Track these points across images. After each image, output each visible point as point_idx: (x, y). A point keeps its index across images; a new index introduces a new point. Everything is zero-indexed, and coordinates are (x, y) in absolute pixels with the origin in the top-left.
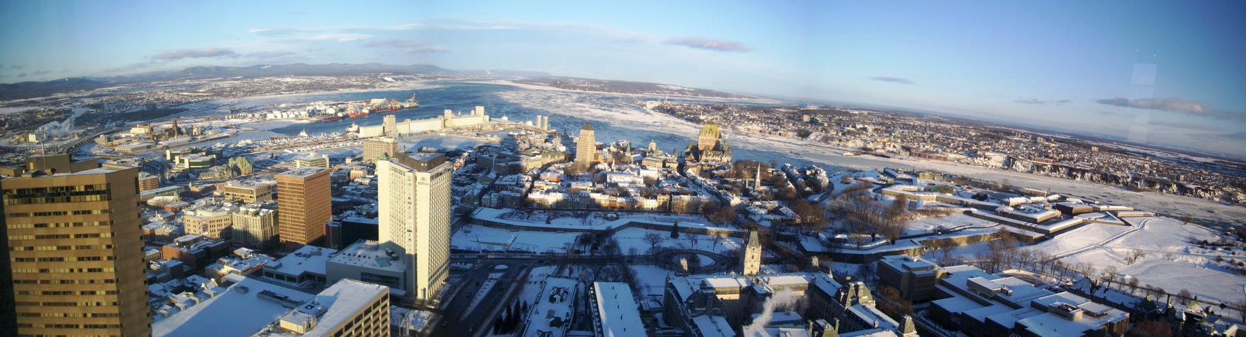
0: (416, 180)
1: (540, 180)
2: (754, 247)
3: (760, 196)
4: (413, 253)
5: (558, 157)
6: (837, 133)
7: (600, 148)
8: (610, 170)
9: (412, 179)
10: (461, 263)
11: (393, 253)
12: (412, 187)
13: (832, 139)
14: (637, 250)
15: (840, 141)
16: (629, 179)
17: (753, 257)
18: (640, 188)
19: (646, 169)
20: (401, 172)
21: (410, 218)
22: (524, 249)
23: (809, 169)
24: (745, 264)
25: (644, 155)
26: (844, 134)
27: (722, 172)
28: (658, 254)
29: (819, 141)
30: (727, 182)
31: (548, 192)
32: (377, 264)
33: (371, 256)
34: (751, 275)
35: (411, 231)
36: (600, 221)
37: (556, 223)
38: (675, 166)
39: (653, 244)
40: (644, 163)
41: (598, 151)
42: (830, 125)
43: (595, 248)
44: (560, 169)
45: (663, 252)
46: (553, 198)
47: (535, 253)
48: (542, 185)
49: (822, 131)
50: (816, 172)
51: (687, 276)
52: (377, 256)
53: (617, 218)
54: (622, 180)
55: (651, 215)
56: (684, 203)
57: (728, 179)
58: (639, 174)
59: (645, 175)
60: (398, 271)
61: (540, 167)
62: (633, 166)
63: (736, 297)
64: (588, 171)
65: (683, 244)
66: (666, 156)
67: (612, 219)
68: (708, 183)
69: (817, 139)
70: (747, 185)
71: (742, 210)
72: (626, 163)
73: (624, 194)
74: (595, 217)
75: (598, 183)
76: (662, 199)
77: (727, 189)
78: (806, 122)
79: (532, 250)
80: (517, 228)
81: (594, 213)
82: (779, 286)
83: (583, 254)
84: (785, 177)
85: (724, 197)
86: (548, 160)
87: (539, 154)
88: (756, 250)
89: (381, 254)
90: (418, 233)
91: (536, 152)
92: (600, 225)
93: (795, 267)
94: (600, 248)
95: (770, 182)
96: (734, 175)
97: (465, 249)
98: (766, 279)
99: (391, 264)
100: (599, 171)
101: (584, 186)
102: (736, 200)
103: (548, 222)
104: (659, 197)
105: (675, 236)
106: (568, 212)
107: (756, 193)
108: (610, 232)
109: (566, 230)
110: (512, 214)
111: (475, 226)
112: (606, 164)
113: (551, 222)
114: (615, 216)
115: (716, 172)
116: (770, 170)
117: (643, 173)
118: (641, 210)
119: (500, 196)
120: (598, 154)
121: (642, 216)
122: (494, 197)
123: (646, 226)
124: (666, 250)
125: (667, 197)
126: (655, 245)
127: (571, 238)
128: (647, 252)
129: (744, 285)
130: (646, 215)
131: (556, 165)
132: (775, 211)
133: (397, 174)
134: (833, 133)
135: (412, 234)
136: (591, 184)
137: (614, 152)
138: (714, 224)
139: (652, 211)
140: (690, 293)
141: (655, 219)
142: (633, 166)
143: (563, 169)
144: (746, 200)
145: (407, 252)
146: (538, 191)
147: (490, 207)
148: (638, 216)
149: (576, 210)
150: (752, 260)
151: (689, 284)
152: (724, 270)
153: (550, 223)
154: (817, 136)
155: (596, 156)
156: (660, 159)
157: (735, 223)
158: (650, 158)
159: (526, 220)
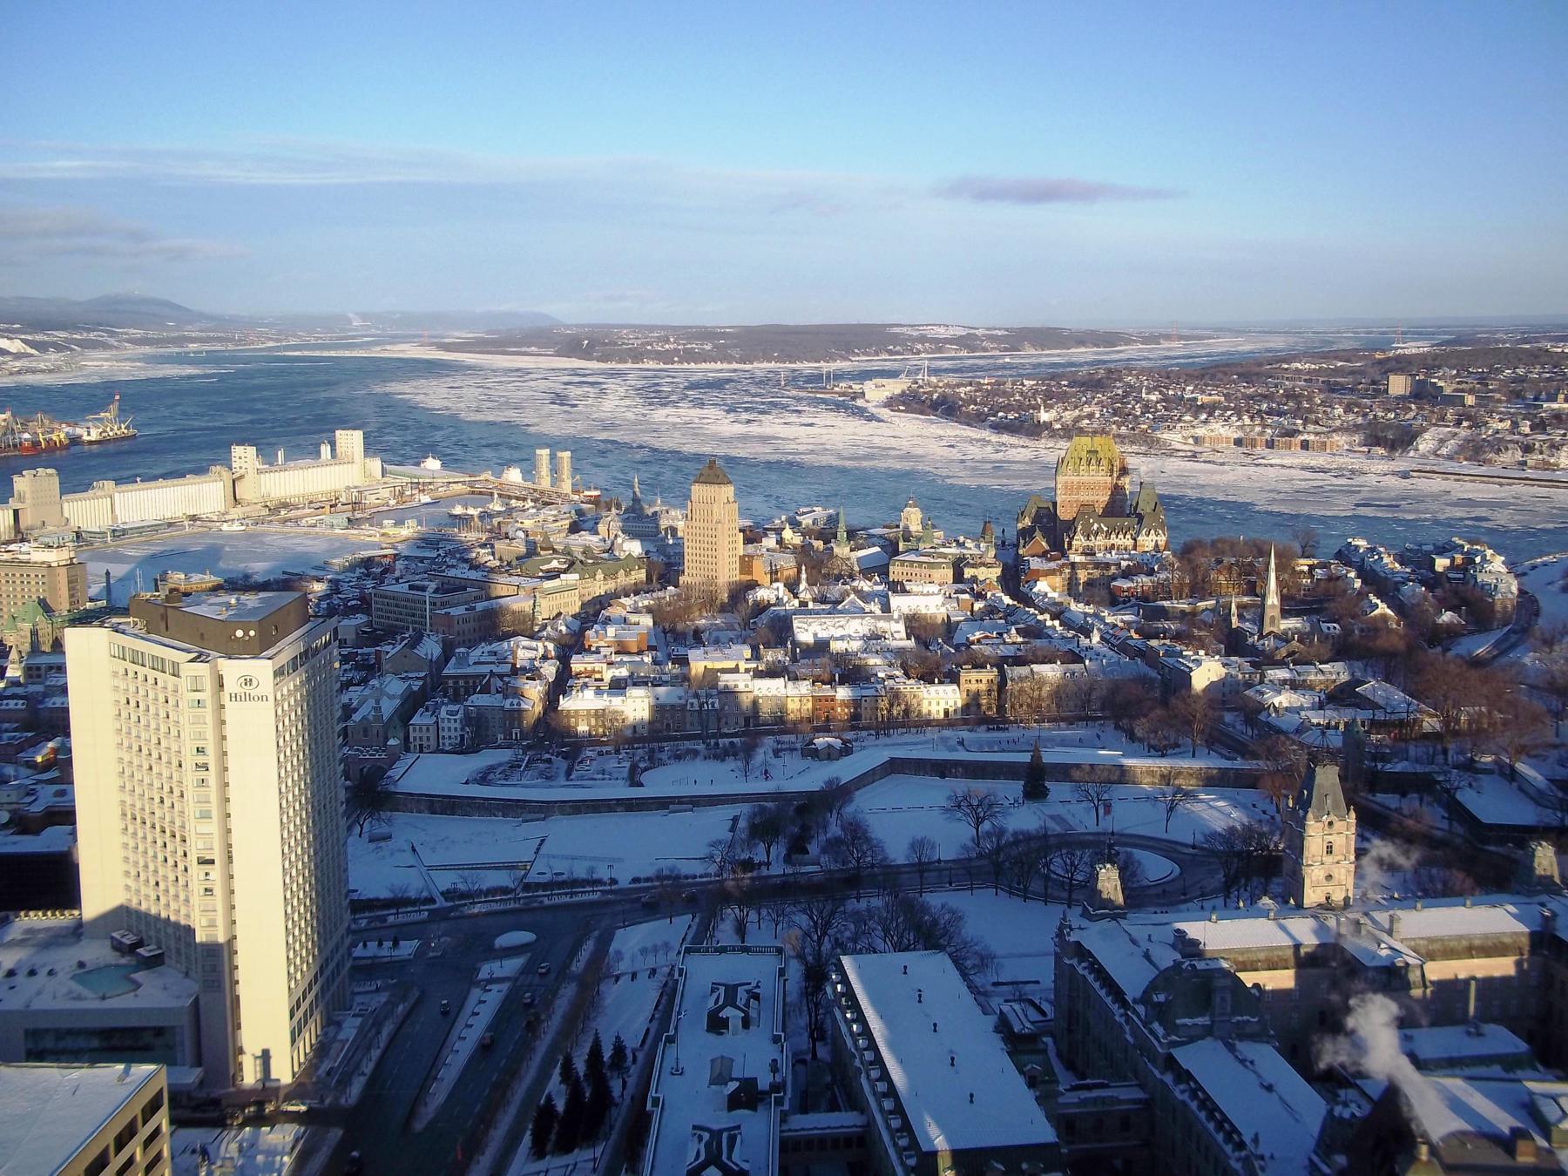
0: (222, 686)
1: (588, 651)
2: (1333, 818)
3: (1284, 652)
4: (221, 939)
5: (627, 574)
6: (1515, 425)
7: (752, 536)
8: (796, 602)
9: (208, 684)
10: (380, 944)
11: (140, 944)
12: (208, 714)
13: (1498, 445)
14: (933, 847)
15: (1528, 449)
16: (858, 627)
17: (1330, 850)
18: (900, 652)
19: (904, 591)
20: (159, 665)
21: (205, 816)
22: (581, 872)
23: (1442, 551)
24: (1306, 871)
25: (891, 549)
26: (1540, 426)
27: (1144, 581)
28: (999, 849)
29: (1450, 458)
30: (1163, 614)
31: (618, 686)
32: (86, 992)
33: (57, 968)
34: (1327, 906)
35: (212, 862)
36: (793, 762)
37: (658, 783)
38: (990, 574)
39: (979, 821)
40: (896, 572)
41: (751, 548)
42: (1483, 401)
43: (797, 848)
44: (636, 611)
45: (1016, 842)
46: (636, 707)
47: (614, 881)
48: (597, 667)
49: (1458, 424)
50: (1469, 561)
51: (1123, 916)
52: (81, 965)
53: (846, 751)
54: (838, 633)
55: (947, 733)
56: (1047, 689)
57: (1166, 604)
58: (886, 608)
59: (906, 611)
60: (174, 1004)
61: (576, 608)
62: (866, 586)
63: (1282, 979)
64: (723, 609)
65: (1069, 818)
66: (961, 545)
67: (830, 754)
68: (1109, 620)
69: (1444, 451)
70: (1234, 619)
71: (1223, 693)
72: (838, 578)
73: (850, 672)
74: (776, 753)
75: (768, 646)
76: (979, 680)
77: (1178, 637)
78: (1402, 398)
79: (603, 873)
80: (544, 810)
81: (769, 741)
82: (1431, 940)
83: (764, 872)
84: (1358, 584)
85: (1171, 660)
86: (599, 586)
87: (565, 571)
88: (1338, 825)
89: (96, 952)
90: (237, 868)
91: (555, 564)
92: (810, 778)
93: (1458, 877)
94: (813, 848)
95: (1303, 602)
96: (1186, 590)
97: (384, 894)
98: (1382, 917)
99: (138, 985)
100: (761, 608)
101: (727, 658)
102: (1207, 672)
103: (635, 782)
104: (964, 676)
105: (1035, 791)
106: (688, 745)
107: (1269, 643)
108: (836, 795)
109: (696, 802)
110: (514, 766)
111: (400, 817)
112: (780, 585)
113: (644, 778)
114: (837, 743)
115: (1124, 584)
116: (1303, 565)
117: (899, 603)
118: (912, 722)
119: (467, 713)
120: (751, 557)
121: (921, 737)
122: (449, 717)
123: (941, 769)
124: (1023, 838)
125: (988, 675)
126: (986, 826)
127: (714, 824)
128: (964, 847)
129: (1310, 941)
130: (931, 733)
131: (623, 600)
132: (1340, 696)
133: (146, 670)
134: (1498, 425)
135: (216, 872)
136: (747, 653)
137: (795, 547)
138: (1151, 747)
139: (948, 722)
140: (1151, 974)
141: (961, 743)
142: (866, 586)
143: (649, 610)
144: (1241, 667)
145: (200, 937)
146: (586, 685)
147: (439, 751)
148: (908, 738)
149: (714, 736)
150: (1328, 859)
151: (1134, 942)
152: (1214, 892)
153: (642, 785)
154: (1442, 442)
155: (746, 563)
156: (944, 556)
157: (1217, 740)
158: (912, 557)
159: (562, 780)
